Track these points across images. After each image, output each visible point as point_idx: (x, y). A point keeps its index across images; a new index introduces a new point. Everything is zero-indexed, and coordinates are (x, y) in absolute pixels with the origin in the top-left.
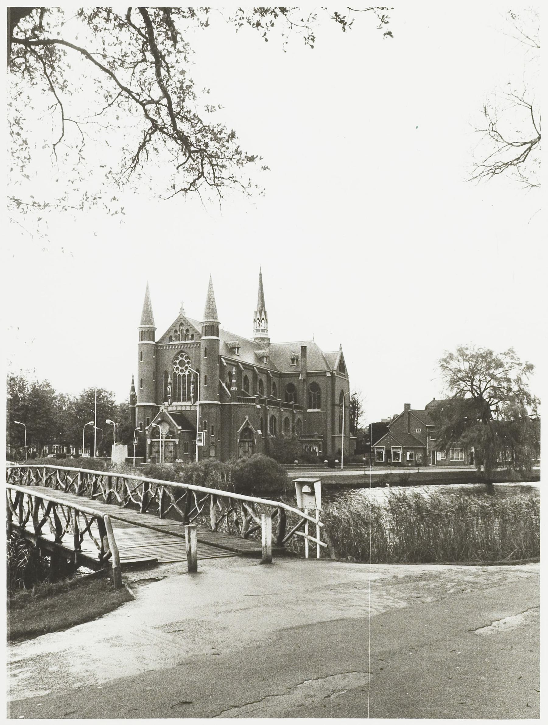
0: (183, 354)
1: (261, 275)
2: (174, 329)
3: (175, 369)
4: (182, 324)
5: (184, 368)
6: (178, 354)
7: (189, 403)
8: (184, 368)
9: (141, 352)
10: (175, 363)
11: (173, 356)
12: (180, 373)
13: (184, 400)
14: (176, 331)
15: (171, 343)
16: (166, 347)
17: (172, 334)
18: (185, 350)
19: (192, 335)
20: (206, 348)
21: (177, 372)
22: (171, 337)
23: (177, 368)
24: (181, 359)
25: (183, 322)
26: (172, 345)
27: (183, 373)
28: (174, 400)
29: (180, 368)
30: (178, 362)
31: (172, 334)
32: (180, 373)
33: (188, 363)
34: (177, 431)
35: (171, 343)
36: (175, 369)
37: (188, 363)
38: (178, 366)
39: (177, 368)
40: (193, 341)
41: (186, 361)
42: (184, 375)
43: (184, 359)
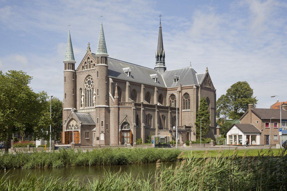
0: (90, 77)
2: (85, 62)
5: (90, 86)
6: (87, 77)
8: (90, 86)
9: (65, 77)
11: (85, 79)
12: (89, 89)
15: (83, 70)
17: (83, 65)
18: (90, 74)
20: (98, 72)
21: (87, 89)
23: (87, 86)
24: (88, 80)
25: (90, 57)
29: (88, 86)
31: (83, 65)
32: (89, 89)
33: (92, 82)
35: (83, 70)
36: (86, 86)
38: (87, 84)
41: (91, 81)
43: (90, 80)
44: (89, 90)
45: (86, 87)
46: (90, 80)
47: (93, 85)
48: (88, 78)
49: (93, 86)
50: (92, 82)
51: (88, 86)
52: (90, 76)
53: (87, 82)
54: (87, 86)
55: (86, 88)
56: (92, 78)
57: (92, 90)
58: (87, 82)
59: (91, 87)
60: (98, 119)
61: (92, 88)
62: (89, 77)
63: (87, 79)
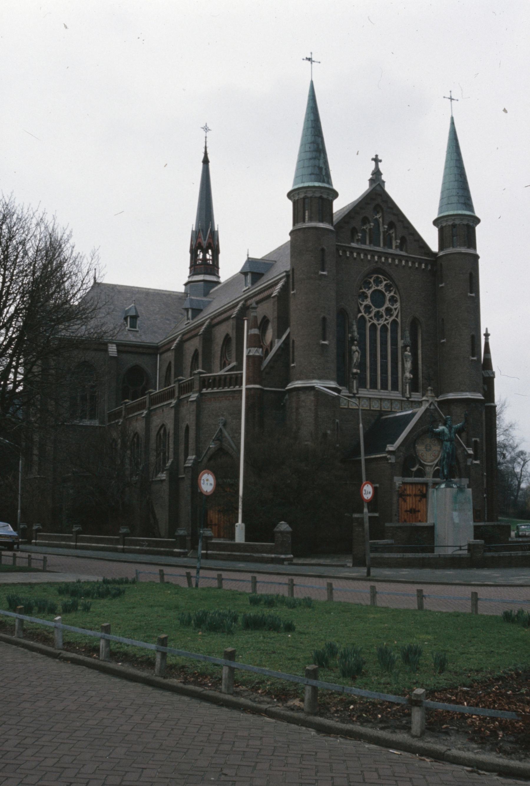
1: (206, 161)
3: (362, 308)
4: (377, 209)
7: (396, 395)
8: (382, 310)
10: (364, 296)
13: (384, 387)
14: (365, 221)
16: (344, 252)
19: (403, 240)
21: (367, 317)
22: (354, 231)
26: (359, 251)
27: (382, 322)
28: (362, 384)
29: (374, 310)
30: (369, 292)
32: (375, 322)
34: (466, 461)
35: (354, 245)
36: (362, 308)
37: (393, 300)
38: (368, 302)
39: (368, 309)
40: (403, 253)
42: (384, 327)
43: (381, 287)
44: (379, 327)
45: (365, 313)
46: (383, 290)
47: (395, 313)
48: (372, 281)
49: (397, 316)
50: (390, 300)
51: (374, 310)
52: (384, 273)
53: (369, 295)
54: (370, 307)
55: (363, 314)
56: (391, 286)
57: (389, 327)
58: (369, 295)
59: (385, 316)
60: (476, 441)
61: (390, 320)
62: (378, 278)
63: (370, 283)
